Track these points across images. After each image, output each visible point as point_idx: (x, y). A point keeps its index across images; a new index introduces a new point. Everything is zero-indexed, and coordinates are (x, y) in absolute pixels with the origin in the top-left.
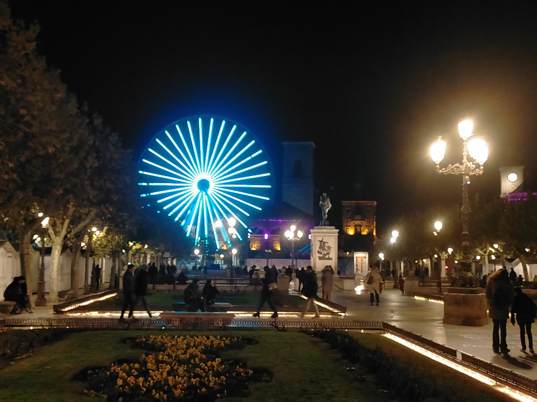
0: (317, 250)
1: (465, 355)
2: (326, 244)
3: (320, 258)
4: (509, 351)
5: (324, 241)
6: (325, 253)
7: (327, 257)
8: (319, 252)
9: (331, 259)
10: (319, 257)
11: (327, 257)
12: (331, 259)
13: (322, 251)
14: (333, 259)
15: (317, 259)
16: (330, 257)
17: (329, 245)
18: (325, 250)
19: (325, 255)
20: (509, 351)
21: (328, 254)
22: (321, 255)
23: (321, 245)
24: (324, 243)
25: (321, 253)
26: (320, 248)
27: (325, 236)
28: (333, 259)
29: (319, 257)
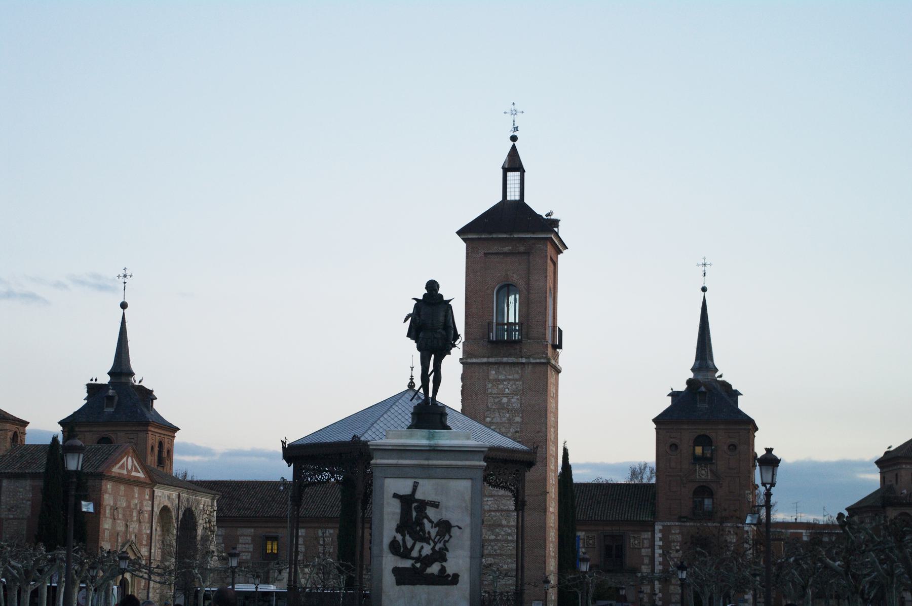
0: (386, 541)
2: (431, 512)
3: (403, 577)
4: (674, 395)
5: (419, 496)
6: (427, 550)
7: (435, 569)
8: (394, 547)
9: (454, 580)
10: (396, 571)
11: (435, 569)
12: (454, 580)
13: (409, 542)
15: (389, 579)
16: (450, 571)
17: (446, 515)
18: (426, 539)
19: (427, 561)
20: (674, 395)
21: (440, 556)
22: (407, 564)
24: (423, 505)
25: (406, 555)
26: (399, 529)
27: (428, 472)
28: (465, 579)
29: (396, 571)
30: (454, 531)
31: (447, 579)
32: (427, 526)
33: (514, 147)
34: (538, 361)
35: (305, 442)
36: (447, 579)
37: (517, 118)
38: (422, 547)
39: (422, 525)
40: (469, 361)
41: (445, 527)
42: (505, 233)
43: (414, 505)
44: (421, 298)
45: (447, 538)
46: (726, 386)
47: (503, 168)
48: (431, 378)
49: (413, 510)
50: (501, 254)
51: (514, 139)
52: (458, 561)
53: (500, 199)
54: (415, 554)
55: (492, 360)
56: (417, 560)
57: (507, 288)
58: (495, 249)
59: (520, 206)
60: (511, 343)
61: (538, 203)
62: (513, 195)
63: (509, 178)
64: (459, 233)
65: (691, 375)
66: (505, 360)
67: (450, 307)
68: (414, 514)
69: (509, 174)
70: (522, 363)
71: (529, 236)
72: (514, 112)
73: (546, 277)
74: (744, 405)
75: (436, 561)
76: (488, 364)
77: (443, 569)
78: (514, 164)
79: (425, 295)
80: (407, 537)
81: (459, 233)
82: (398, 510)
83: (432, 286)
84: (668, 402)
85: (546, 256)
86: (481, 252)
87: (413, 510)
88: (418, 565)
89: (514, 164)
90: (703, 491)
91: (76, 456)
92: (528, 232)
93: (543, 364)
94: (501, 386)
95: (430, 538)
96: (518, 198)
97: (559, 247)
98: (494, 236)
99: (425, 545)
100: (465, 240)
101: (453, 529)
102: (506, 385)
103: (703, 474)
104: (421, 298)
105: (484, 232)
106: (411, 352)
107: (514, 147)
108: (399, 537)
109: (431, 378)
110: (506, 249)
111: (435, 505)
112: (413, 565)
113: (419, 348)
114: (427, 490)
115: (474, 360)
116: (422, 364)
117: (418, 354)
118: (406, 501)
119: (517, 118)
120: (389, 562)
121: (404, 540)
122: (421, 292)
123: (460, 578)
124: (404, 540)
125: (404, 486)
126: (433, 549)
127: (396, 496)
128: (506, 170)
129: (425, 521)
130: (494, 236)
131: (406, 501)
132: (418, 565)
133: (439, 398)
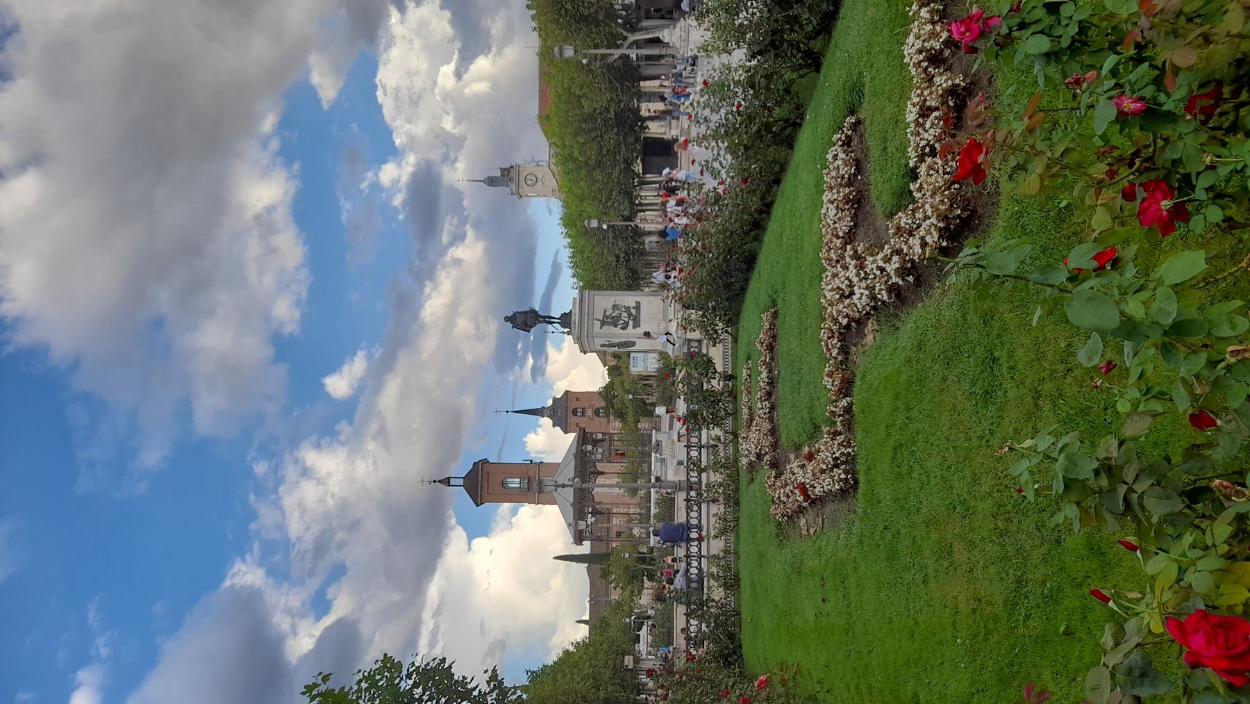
3: (637, 324)
7: (633, 312)
12: (638, 303)
14: (638, 299)
19: (630, 315)
21: (628, 309)
23: (609, 324)
24: (605, 316)
25: (627, 323)
28: (638, 299)
41: (615, 307)
49: (610, 320)
57: (503, 484)
62: (461, 482)
83: (507, 319)
84: (558, 428)
87: (610, 320)
90: (597, 412)
97: (485, 461)
103: (589, 412)
118: (603, 323)
131: (603, 323)
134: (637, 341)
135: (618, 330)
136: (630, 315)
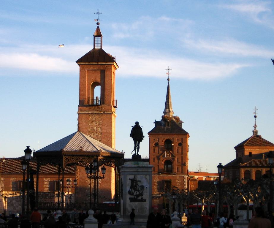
1: (108, 145)
2: (138, 183)
3: (132, 200)
4: (156, 123)
6: (138, 193)
7: (140, 198)
8: (130, 193)
9: (145, 201)
11: (140, 198)
12: (145, 201)
13: (133, 191)
15: (128, 201)
18: (138, 190)
19: (138, 196)
20: (156, 123)
21: (141, 194)
22: (132, 197)
25: (132, 194)
29: (130, 199)
30: (145, 188)
31: (143, 201)
32: (138, 187)
33: (98, 27)
34: (108, 113)
35: (42, 151)
36: (143, 201)
37: (99, 16)
38: (136, 193)
39: (136, 187)
40: (81, 112)
41: (142, 187)
42: (95, 62)
43: (134, 181)
44: (134, 126)
45: (143, 190)
46: (177, 119)
47: (94, 36)
48: (137, 147)
50: (94, 70)
51: (98, 24)
52: (146, 196)
53: (92, 48)
54: (135, 194)
55: (90, 112)
56: (136, 196)
57: (95, 84)
58: (91, 68)
59: (101, 51)
60: (97, 105)
61: (107, 49)
62: (98, 47)
63: (96, 40)
64: (77, 62)
65: (163, 115)
66: (95, 112)
67: (142, 129)
68: (134, 184)
69: (96, 38)
70: (102, 114)
71: (105, 63)
72: (98, 13)
73: (111, 79)
74: (184, 127)
75: (140, 196)
76: (88, 114)
77: (142, 198)
78: (98, 34)
79: (135, 125)
80: (133, 190)
81: (77, 62)
82: (130, 183)
85: (112, 71)
86: (86, 69)
88: (136, 197)
89: (98, 34)
91: (25, 165)
92: (104, 62)
93: (110, 114)
94: (94, 123)
95: (138, 190)
96: (100, 48)
98: (91, 63)
99: (137, 192)
100: (79, 65)
101: (144, 188)
102: (95, 122)
104: (134, 126)
105: (87, 62)
106: (131, 141)
107: (98, 27)
108: (131, 190)
109: (137, 147)
110: (96, 68)
111: (140, 181)
112: (134, 197)
113: (134, 140)
114: (139, 178)
115: (83, 112)
116: (135, 144)
117: (133, 142)
118: (133, 181)
119: (99, 16)
120: (128, 196)
121: (132, 191)
122: (134, 125)
123: (146, 201)
124: (132, 191)
125: (132, 177)
126: (139, 193)
127: (129, 179)
128: (95, 37)
129: (137, 186)
130: (91, 63)
131: (133, 181)
132: (136, 197)
133: (139, 154)
134: (123, 200)
135: (128, 188)
136: (138, 196)
